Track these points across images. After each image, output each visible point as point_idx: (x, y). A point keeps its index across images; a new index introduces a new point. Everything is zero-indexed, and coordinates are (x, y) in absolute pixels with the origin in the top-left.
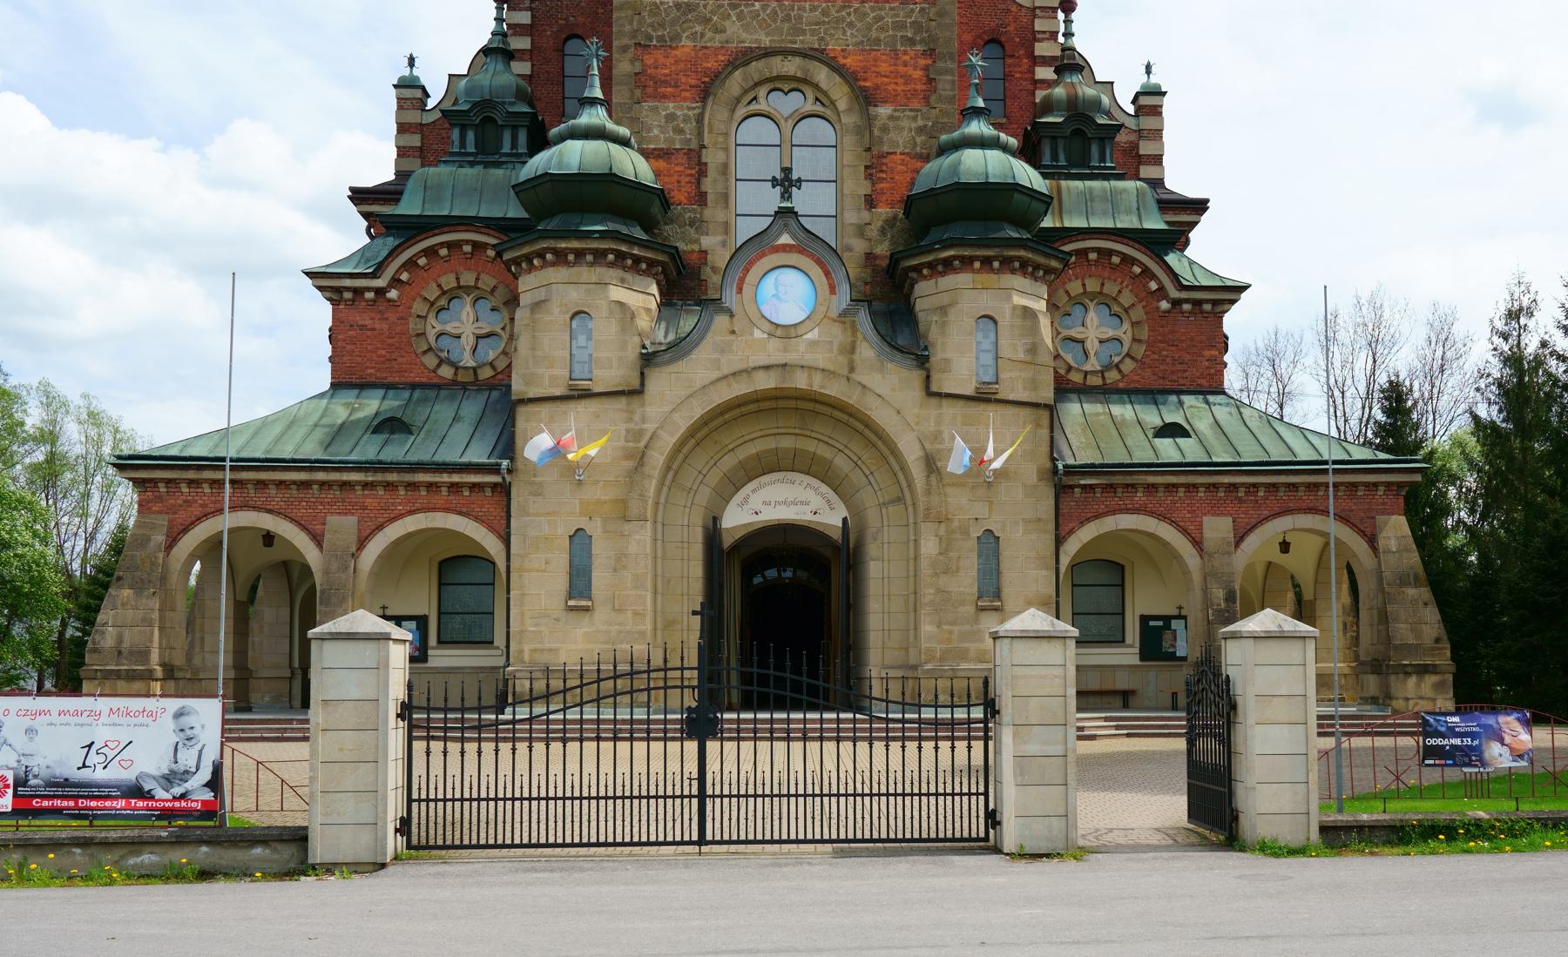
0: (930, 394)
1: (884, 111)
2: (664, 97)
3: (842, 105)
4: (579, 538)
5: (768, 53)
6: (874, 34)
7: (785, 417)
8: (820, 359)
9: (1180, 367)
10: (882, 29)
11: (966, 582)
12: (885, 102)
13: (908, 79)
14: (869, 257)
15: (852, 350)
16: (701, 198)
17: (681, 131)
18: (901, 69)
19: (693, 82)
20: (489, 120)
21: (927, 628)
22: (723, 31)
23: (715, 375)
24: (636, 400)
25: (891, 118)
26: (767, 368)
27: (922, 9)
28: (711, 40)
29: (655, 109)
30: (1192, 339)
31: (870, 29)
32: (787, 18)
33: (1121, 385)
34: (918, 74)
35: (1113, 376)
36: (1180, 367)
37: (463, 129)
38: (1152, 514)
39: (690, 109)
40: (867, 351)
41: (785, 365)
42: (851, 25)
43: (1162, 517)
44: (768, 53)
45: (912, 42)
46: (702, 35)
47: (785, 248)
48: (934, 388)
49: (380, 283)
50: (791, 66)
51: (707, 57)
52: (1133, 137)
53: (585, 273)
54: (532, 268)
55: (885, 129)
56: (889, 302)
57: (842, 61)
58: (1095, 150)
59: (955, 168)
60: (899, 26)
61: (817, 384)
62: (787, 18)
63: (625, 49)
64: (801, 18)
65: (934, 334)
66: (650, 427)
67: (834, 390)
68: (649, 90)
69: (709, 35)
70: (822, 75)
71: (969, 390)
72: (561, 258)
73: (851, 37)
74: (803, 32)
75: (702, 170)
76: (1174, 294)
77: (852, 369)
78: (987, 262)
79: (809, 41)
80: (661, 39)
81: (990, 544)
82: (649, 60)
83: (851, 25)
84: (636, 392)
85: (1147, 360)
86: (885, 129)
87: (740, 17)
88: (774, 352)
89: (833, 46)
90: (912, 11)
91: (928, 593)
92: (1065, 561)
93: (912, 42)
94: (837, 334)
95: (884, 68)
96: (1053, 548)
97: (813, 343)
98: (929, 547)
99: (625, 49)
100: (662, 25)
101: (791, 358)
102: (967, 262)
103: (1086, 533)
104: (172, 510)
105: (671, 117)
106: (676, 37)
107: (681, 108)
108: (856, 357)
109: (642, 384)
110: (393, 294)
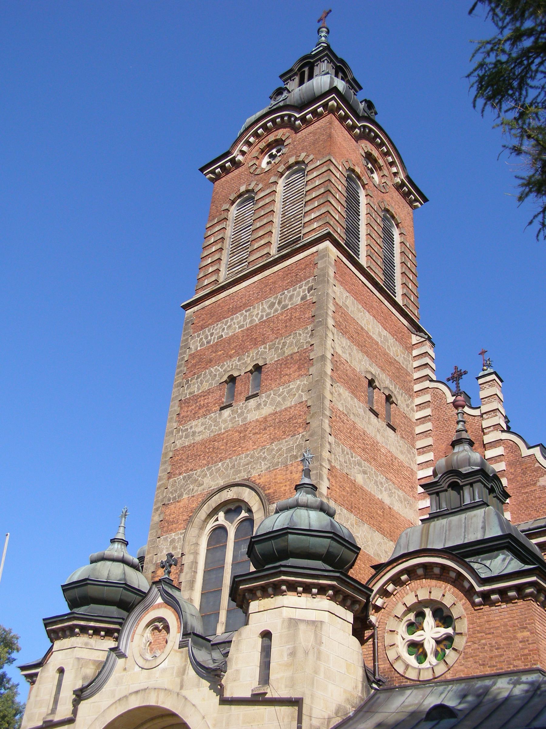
0: (224, 701)
6: (276, 460)
9: (496, 652)
18: (288, 476)
19: (185, 518)
22: (202, 485)
23: (113, 701)
26: (137, 692)
27: (303, 436)
28: (197, 490)
30: (505, 625)
31: (274, 458)
33: (449, 676)
35: (441, 669)
36: (496, 652)
39: (181, 534)
41: (145, 689)
42: (265, 458)
46: (193, 489)
47: (159, 606)
48: (228, 694)
51: (193, 501)
57: (258, 481)
60: (290, 450)
62: (233, 467)
64: (239, 463)
68: (165, 529)
69: (196, 488)
71: (247, 694)
73: (264, 466)
74: (240, 472)
77: (182, 687)
79: (244, 475)
80: (174, 498)
82: (168, 512)
83: (265, 458)
85: (469, 650)
90: (297, 439)
93: (296, 457)
100: (176, 491)
105: (173, 541)
106: (181, 495)
107: (178, 534)
108: (185, 677)
109: (75, 712)
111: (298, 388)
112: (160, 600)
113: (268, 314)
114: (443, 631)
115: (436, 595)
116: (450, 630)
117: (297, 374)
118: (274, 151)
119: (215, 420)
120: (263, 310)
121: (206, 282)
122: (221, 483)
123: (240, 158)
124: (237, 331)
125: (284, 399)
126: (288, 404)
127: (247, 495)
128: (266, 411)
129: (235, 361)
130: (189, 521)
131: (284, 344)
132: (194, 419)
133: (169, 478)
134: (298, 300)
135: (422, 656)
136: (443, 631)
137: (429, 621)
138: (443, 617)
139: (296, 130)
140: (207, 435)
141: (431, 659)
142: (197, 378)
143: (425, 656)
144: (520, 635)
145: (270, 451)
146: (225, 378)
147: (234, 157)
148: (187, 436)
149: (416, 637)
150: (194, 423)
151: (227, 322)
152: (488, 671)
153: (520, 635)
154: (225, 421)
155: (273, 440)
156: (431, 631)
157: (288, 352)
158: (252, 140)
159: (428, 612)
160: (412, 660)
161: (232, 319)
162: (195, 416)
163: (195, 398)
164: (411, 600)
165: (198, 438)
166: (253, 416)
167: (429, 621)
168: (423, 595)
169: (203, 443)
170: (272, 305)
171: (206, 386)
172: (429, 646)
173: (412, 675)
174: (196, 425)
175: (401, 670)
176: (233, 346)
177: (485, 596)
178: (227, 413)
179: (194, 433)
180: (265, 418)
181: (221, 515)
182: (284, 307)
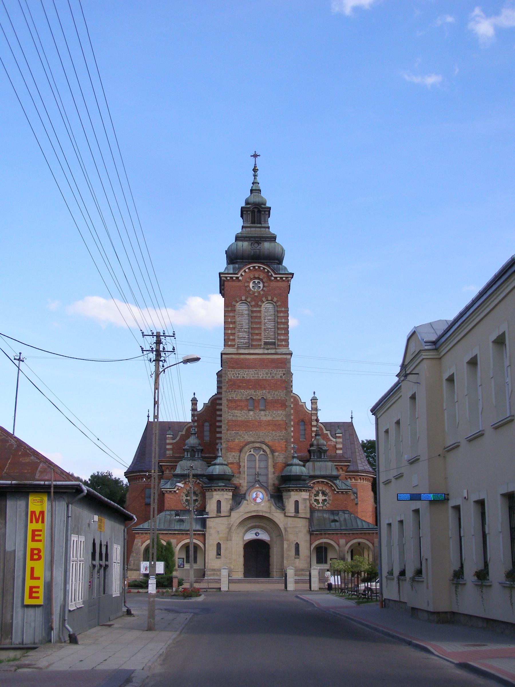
1: (277, 454)
2: (232, 452)
3: (268, 453)
4: (219, 545)
5: (254, 442)
7: (258, 520)
8: (264, 509)
10: (276, 437)
11: (293, 552)
12: (277, 452)
13: (282, 447)
14: (274, 484)
15: (271, 507)
16: (240, 473)
17: (235, 458)
20: (193, 450)
21: (285, 562)
24: (229, 518)
25: (278, 455)
29: (230, 454)
32: (257, 435)
34: (284, 446)
35: (324, 507)
37: (187, 452)
38: (329, 539)
40: (273, 508)
43: (331, 540)
44: (254, 442)
45: (282, 439)
47: (258, 488)
48: (286, 515)
49: (175, 490)
50: (257, 445)
52: (335, 443)
53: (219, 493)
54: (209, 491)
55: (277, 458)
56: (278, 496)
58: (323, 455)
59: (291, 471)
60: (280, 436)
61: (264, 514)
63: (224, 442)
65: (286, 504)
66: (232, 523)
67: (267, 515)
70: (264, 447)
72: (215, 490)
75: (240, 467)
76: (337, 490)
78: (296, 490)
79: (261, 439)
81: (297, 546)
84: (230, 516)
86: (277, 458)
87: (248, 435)
88: (255, 508)
89: (266, 441)
91: (285, 555)
92: (312, 548)
93: (282, 439)
94: (268, 504)
95: (277, 445)
96: (309, 546)
97: (263, 506)
98: (285, 546)
99: (224, 442)
100: (232, 437)
101: (259, 509)
102: (293, 490)
103: (317, 543)
104: (142, 538)
105: (234, 456)
106: (234, 439)
110: (177, 492)
111: (282, 414)
112: (258, 486)
113: (266, 377)
114: (324, 498)
115: (324, 489)
116: (326, 498)
117: (281, 408)
118: (256, 281)
119: (246, 414)
120: (263, 373)
121: (230, 343)
122: (253, 440)
123: (240, 278)
124: (252, 378)
125: (276, 416)
126: (278, 419)
127: (264, 447)
128: (269, 418)
129: (252, 392)
130: (240, 451)
131: (274, 394)
132: (236, 410)
133: (228, 431)
134: (279, 377)
135: (318, 503)
136: (324, 498)
137: (320, 495)
138: (324, 494)
139: (271, 280)
140: (243, 418)
141: (321, 505)
142: (235, 392)
143: (319, 503)
144: (345, 502)
145: (272, 434)
146: (249, 398)
147: (238, 277)
148: (233, 416)
149: (317, 498)
150: (236, 411)
151: (246, 371)
152: (336, 509)
153: (345, 502)
154: (251, 416)
155: (273, 430)
156: (321, 498)
157: (276, 398)
158: (247, 270)
159: (320, 492)
160: (315, 503)
161: (248, 371)
162: (236, 408)
163: (235, 401)
164: (317, 489)
165: (239, 419)
166: (264, 418)
167: (320, 495)
168: (320, 488)
169: (242, 421)
170: (267, 374)
171: (239, 397)
172: (320, 501)
173: (317, 508)
174: (237, 413)
175: (314, 506)
176: (250, 384)
177: (338, 492)
178: (251, 413)
179: (237, 416)
180: (269, 421)
181: (252, 450)
182: (273, 377)
